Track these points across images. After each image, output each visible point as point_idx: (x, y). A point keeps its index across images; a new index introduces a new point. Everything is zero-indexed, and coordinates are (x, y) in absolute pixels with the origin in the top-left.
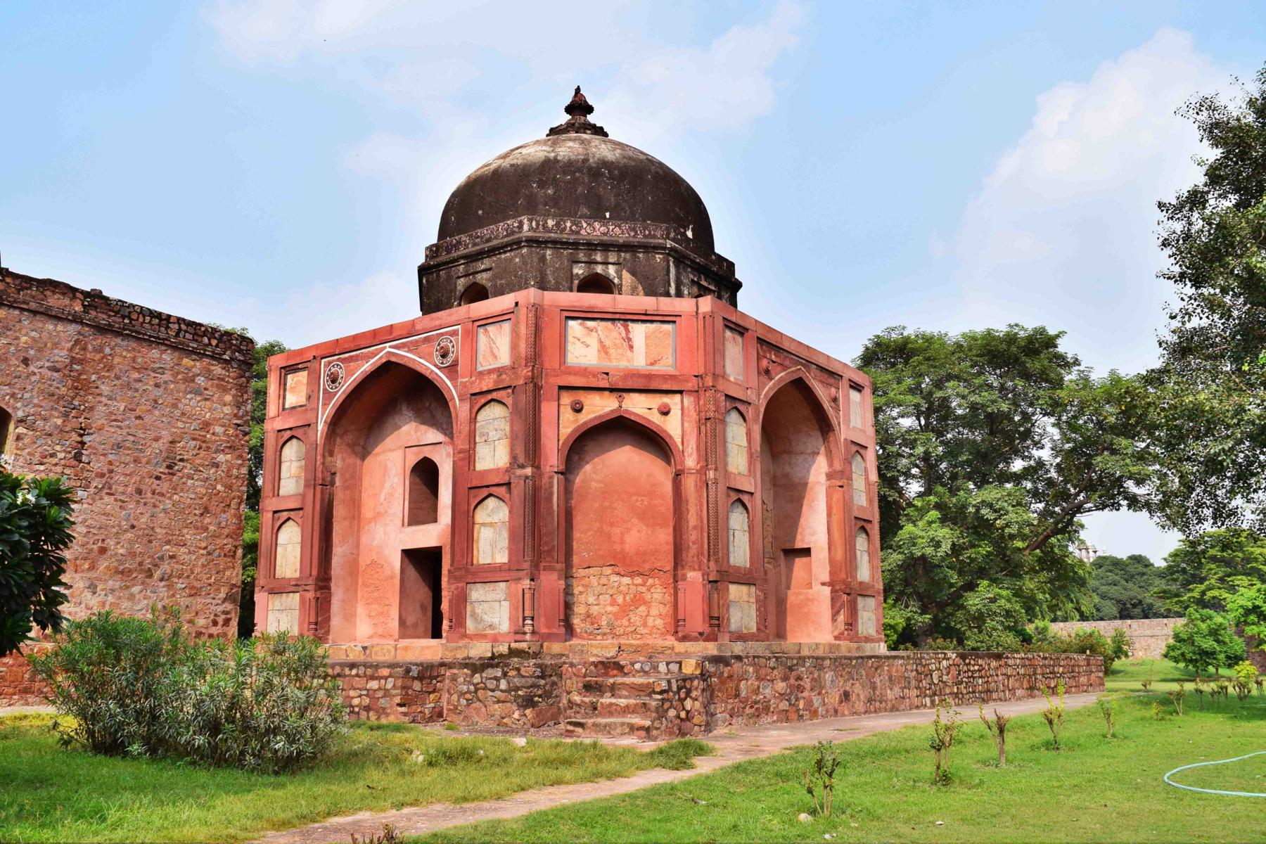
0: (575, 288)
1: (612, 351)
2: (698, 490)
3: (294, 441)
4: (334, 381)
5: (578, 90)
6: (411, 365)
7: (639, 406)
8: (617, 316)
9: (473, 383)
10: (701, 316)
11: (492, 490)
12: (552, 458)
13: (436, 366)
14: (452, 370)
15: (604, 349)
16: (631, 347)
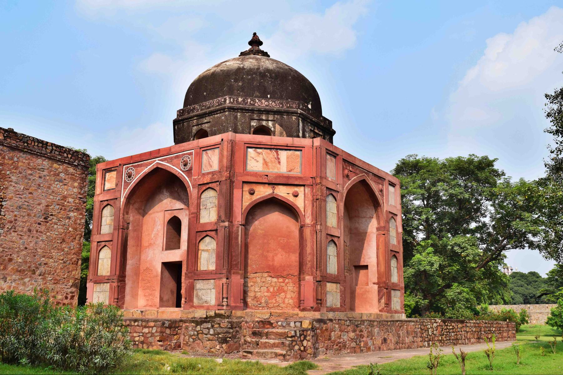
0: (252, 132)
1: (270, 164)
2: (312, 235)
3: (109, 206)
4: (129, 177)
5: (255, 34)
6: (168, 169)
7: (283, 192)
8: (273, 147)
9: (200, 179)
10: (315, 148)
11: (208, 233)
12: (239, 218)
13: (181, 170)
14: (189, 172)
15: (265, 163)
16: (279, 163)
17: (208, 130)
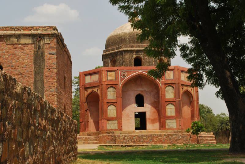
2: (196, 104)
17: (142, 57)
